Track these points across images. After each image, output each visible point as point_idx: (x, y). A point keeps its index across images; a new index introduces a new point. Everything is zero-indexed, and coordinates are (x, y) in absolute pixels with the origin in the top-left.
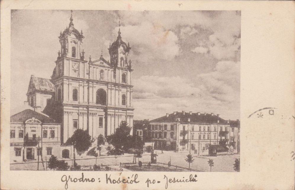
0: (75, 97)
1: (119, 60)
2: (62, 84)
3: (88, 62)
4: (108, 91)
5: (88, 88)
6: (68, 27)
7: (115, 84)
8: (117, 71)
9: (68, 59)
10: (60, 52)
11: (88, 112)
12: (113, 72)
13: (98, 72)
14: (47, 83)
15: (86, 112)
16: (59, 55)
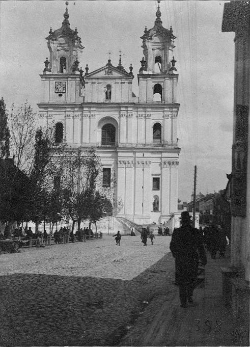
5: (82, 119)
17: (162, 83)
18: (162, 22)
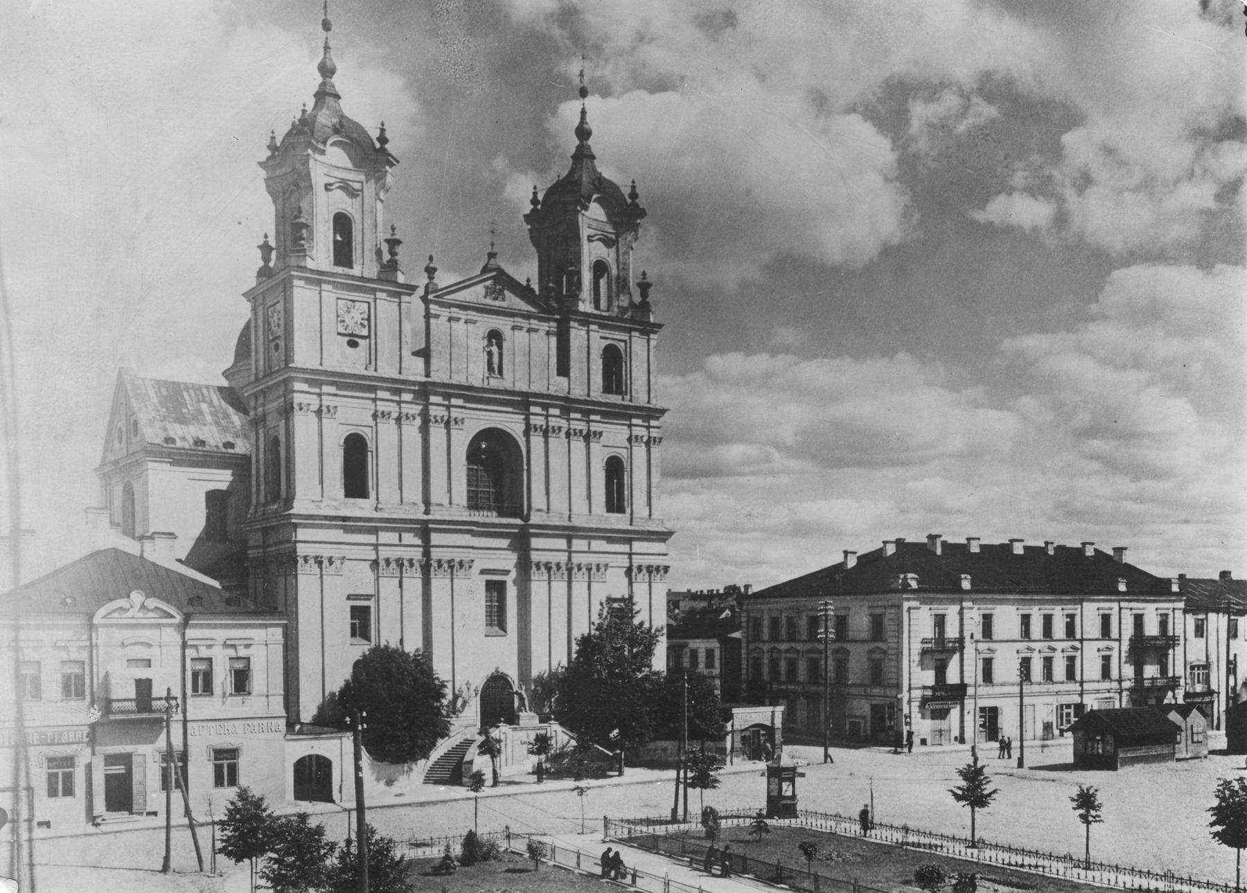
0: (356, 483)
1: (587, 277)
2: (287, 411)
3: (420, 292)
4: (532, 439)
5: (425, 430)
6: (309, 108)
7: (568, 405)
8: (577, 335)
9: (317, 279)
10: (273, 243)
11: (427, 554)
12: (553, 340)
13: (477, 343)
14: (204, 407)
15: (417, 554)
16: (266, 259)
17: (623, 344)
18: (593, 157)
